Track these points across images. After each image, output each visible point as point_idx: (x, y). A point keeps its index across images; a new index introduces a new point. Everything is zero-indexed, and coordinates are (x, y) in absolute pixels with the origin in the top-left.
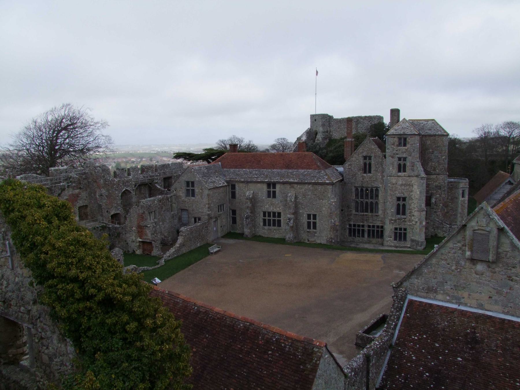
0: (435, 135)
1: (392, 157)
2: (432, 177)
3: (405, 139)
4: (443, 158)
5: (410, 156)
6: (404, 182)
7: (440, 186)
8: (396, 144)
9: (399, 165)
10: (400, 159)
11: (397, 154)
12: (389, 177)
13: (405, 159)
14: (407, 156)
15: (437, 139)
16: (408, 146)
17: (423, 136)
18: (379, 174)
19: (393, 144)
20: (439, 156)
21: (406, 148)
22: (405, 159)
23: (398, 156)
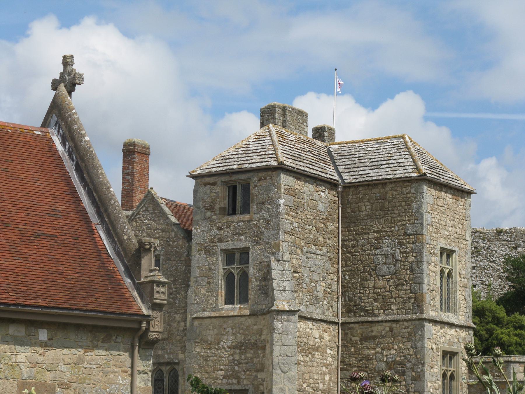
0: (383, 183)
1: (208, 251)
2: (376, 329)
3: (246, 188)
4: (411, 259)
5: (257, 243)
6: (240, 338)
7: (401, 363)
8: (217, 207)
9: (229, 278)
10: (230, 256)
11: (220, 241)
12: (196, 323)
13: (245, 252)
14: (249, 244)
15: (389, 195)
16: (254, 208)
17: (347, 187)
18: (178, 317)
19: (211, 208)
20: (398, 256)
21: (246, 217)
22: (245, 252)
23: (223, 246)
